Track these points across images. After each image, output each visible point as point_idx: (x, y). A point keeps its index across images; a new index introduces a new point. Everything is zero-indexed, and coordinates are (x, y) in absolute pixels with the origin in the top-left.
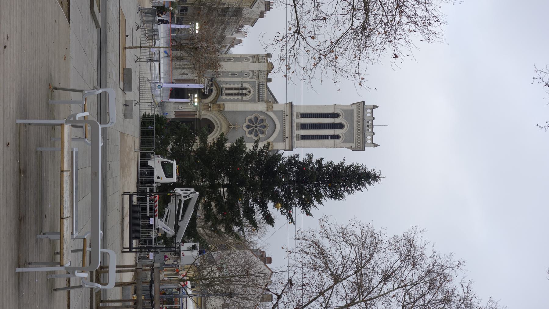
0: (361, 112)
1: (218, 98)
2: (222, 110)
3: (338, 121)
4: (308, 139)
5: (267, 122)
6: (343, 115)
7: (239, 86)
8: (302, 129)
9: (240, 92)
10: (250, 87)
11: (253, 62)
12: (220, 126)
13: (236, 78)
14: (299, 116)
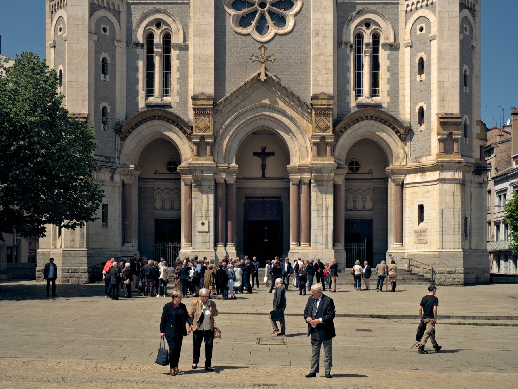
2: (211, 102)
13: (118, 62)
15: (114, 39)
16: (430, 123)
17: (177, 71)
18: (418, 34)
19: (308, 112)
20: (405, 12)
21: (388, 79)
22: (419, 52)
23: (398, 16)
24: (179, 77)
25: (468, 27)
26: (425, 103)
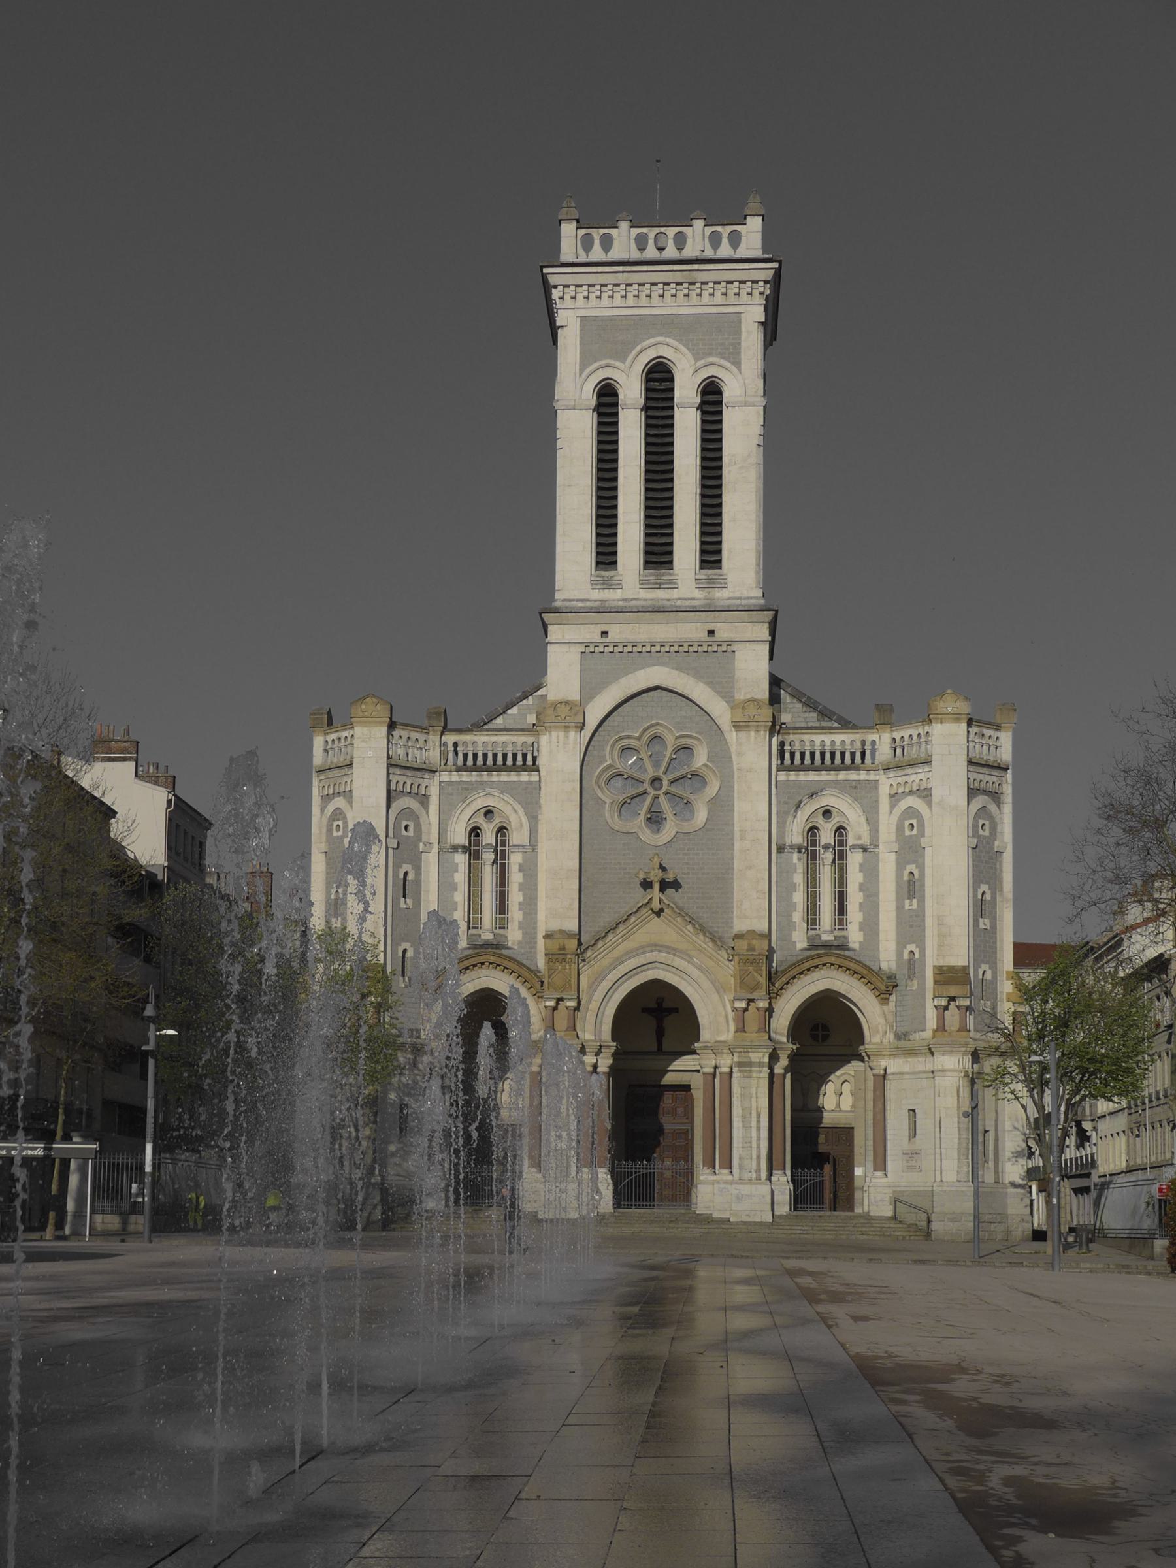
0: (592, 279)
1: (520, 964)
3: (632, 392)
4: (720, 533)
5: (632, 726)
6: (607, 366)
7: (460, 859)
8: (669, 563)
9: (488, 856)
10: (468, 813)
11: (348, 795)
12: (650, 956)
14: (611, 579)
15: (420, 840)
16: (923, 977)
17: (519, 891)
18: (906, 834)
19: (728, 960)
20: (888, 796)
21: (860, 903)
22: (909, 863)
23: (877, 801)
24: (521, 899)
25: (987, 823)
26: (917, 946)
